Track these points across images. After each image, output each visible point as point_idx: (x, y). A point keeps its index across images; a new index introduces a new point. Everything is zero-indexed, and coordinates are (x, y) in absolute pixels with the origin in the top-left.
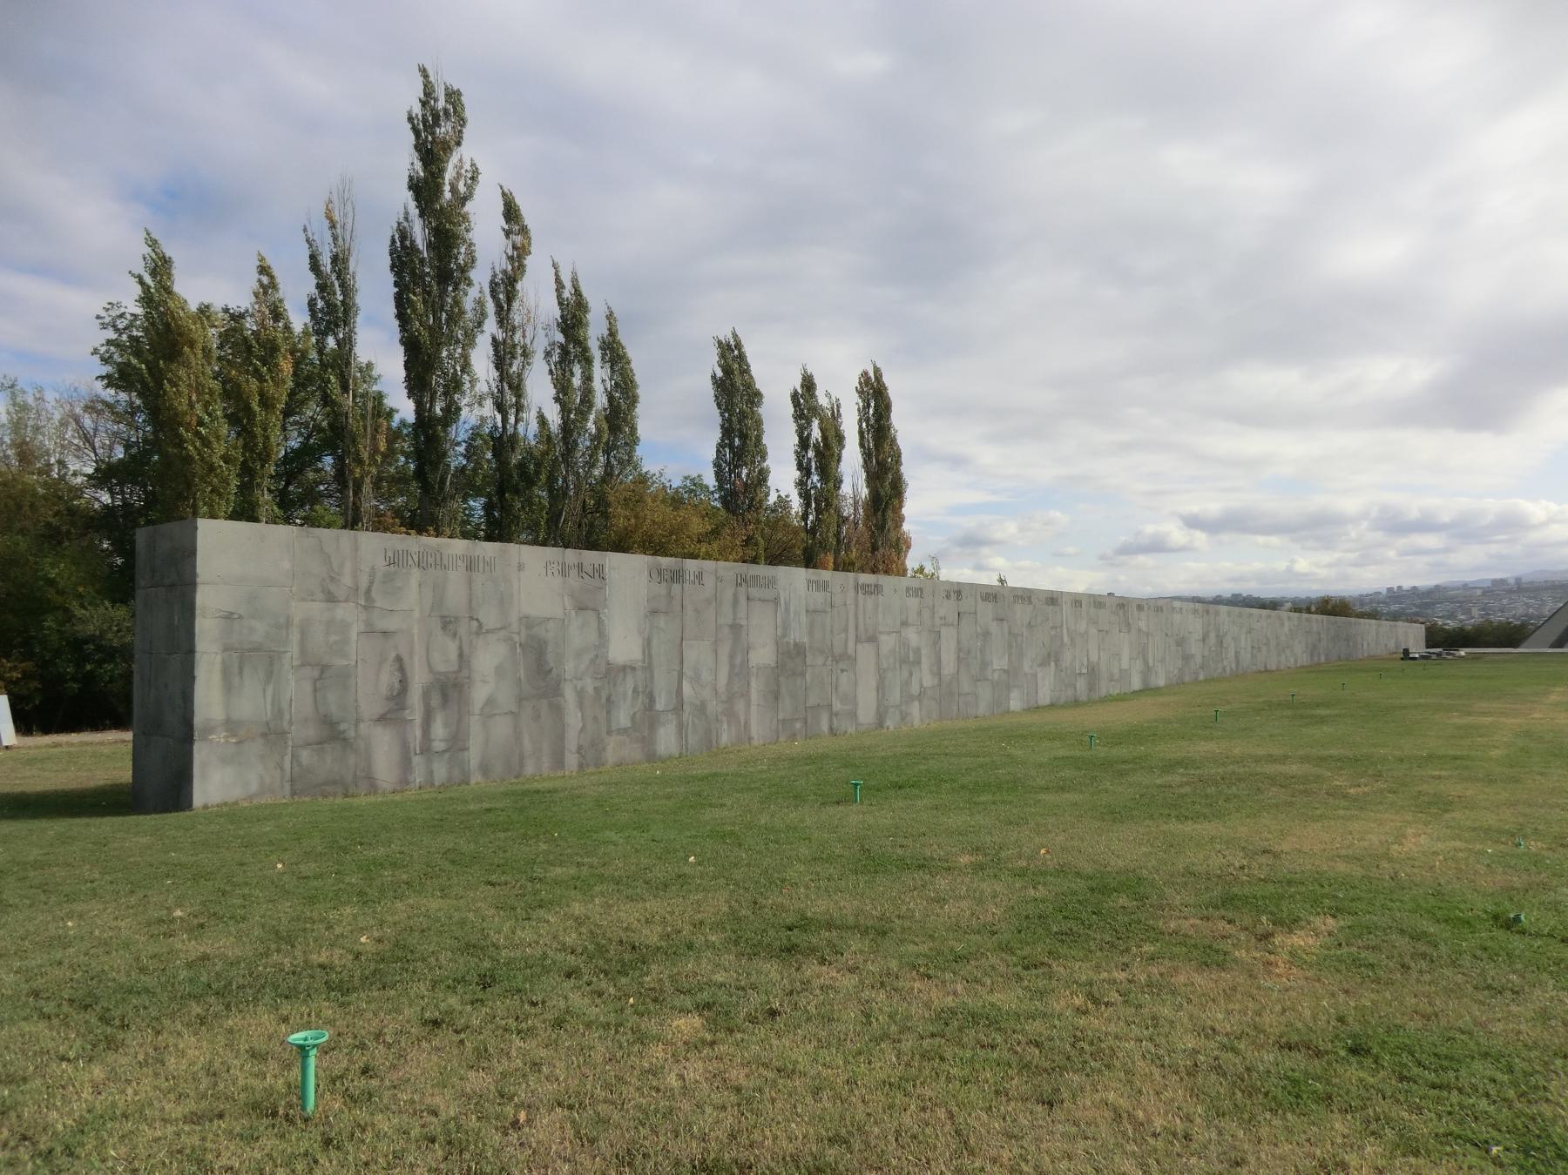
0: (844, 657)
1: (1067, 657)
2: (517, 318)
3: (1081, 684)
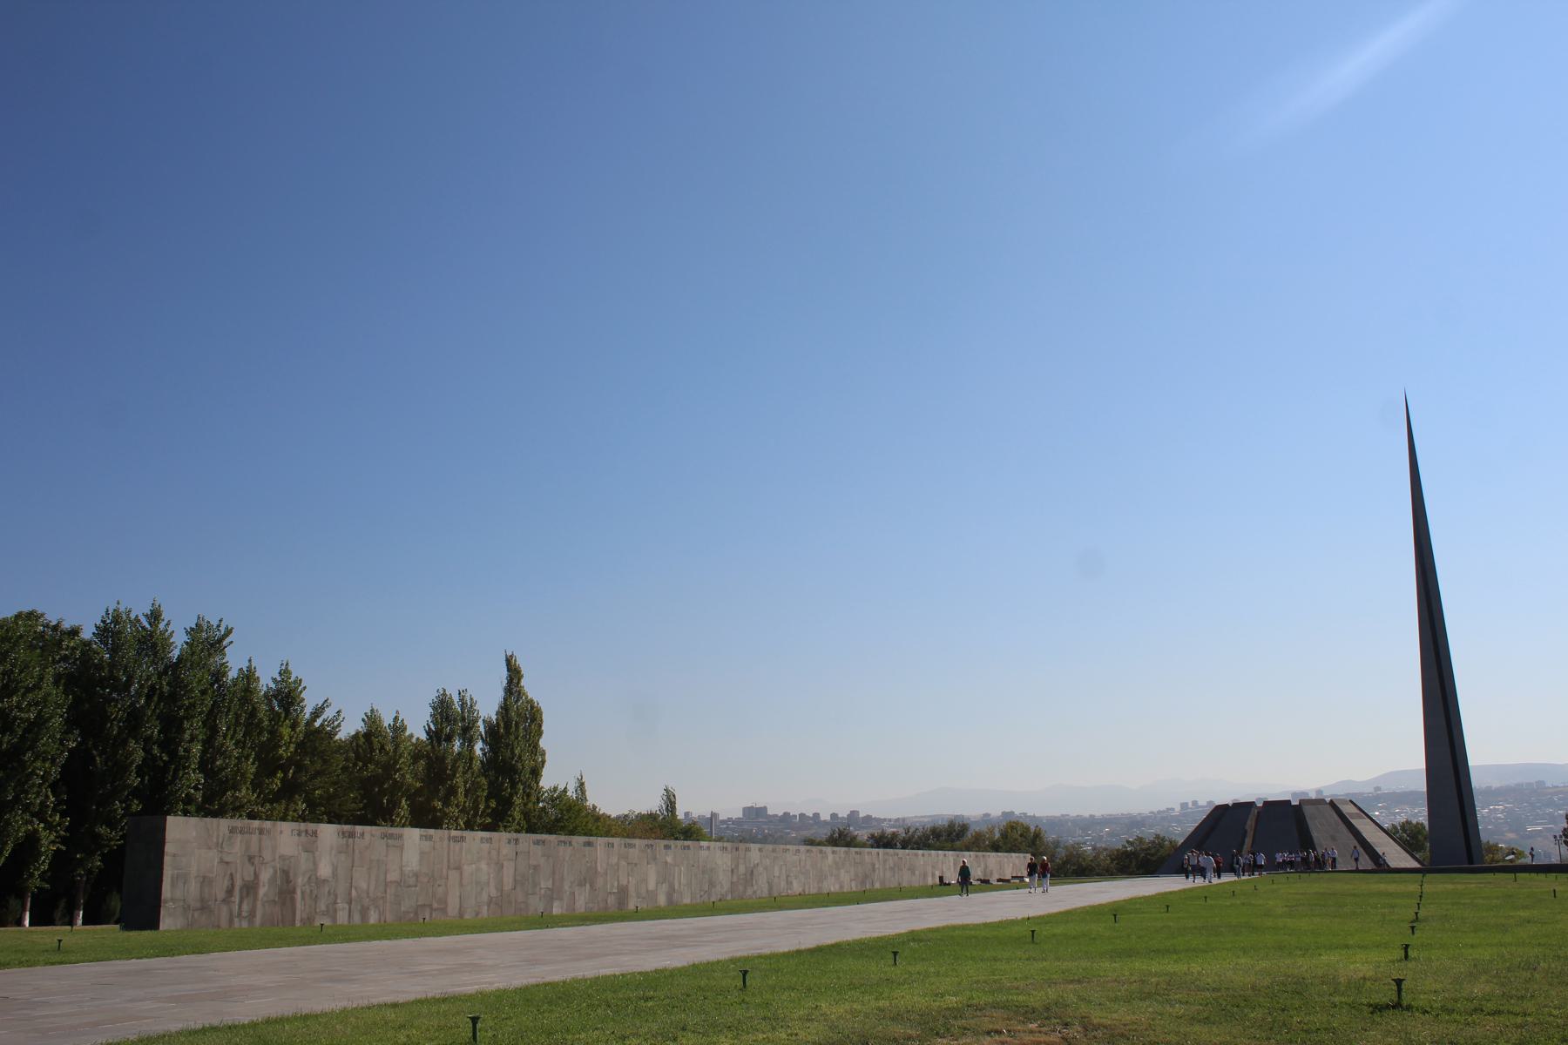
1: (600, 882)
3: (611, 900)
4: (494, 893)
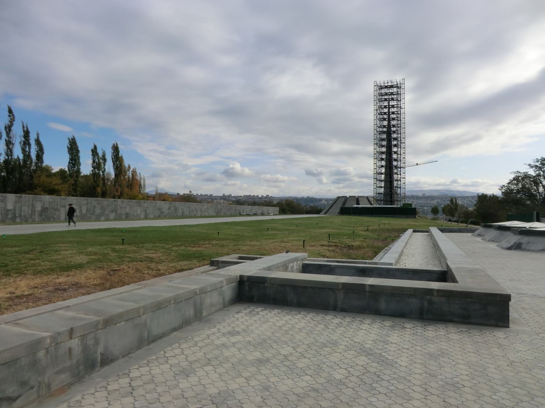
0: (57, 209)
1: (119, 211)
2: (11, 135)
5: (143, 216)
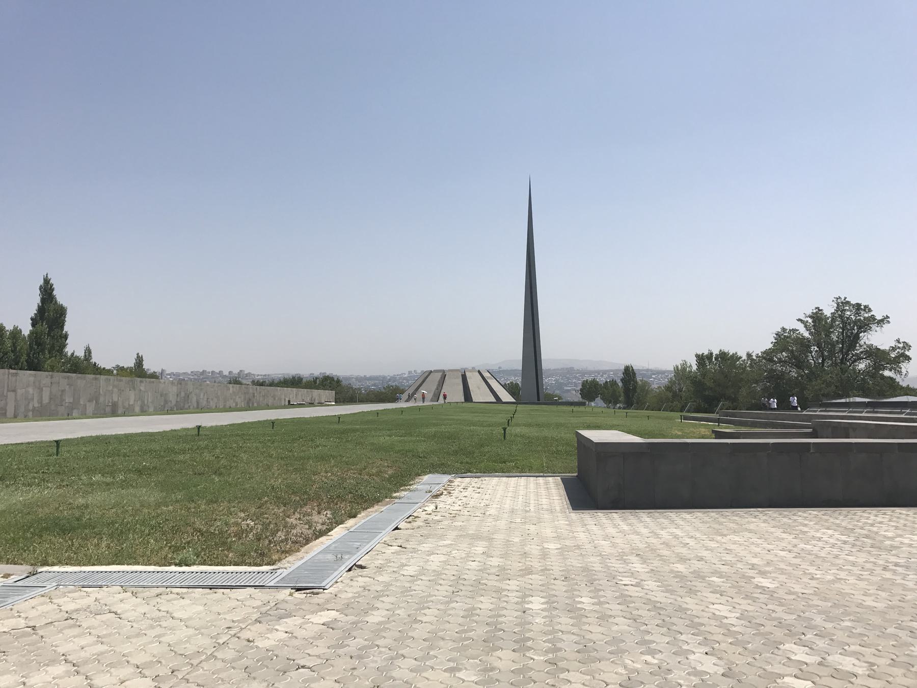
1: (101, 399)
4: (36, 405)
5: (137, 409)
